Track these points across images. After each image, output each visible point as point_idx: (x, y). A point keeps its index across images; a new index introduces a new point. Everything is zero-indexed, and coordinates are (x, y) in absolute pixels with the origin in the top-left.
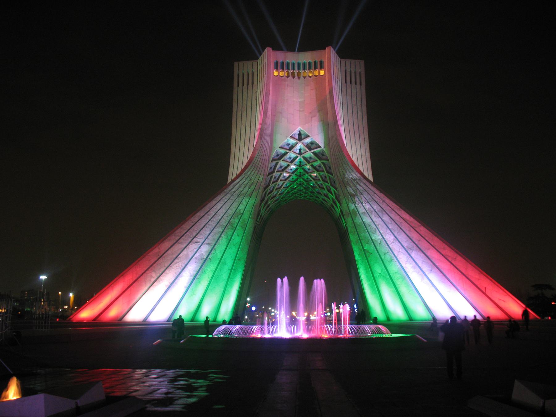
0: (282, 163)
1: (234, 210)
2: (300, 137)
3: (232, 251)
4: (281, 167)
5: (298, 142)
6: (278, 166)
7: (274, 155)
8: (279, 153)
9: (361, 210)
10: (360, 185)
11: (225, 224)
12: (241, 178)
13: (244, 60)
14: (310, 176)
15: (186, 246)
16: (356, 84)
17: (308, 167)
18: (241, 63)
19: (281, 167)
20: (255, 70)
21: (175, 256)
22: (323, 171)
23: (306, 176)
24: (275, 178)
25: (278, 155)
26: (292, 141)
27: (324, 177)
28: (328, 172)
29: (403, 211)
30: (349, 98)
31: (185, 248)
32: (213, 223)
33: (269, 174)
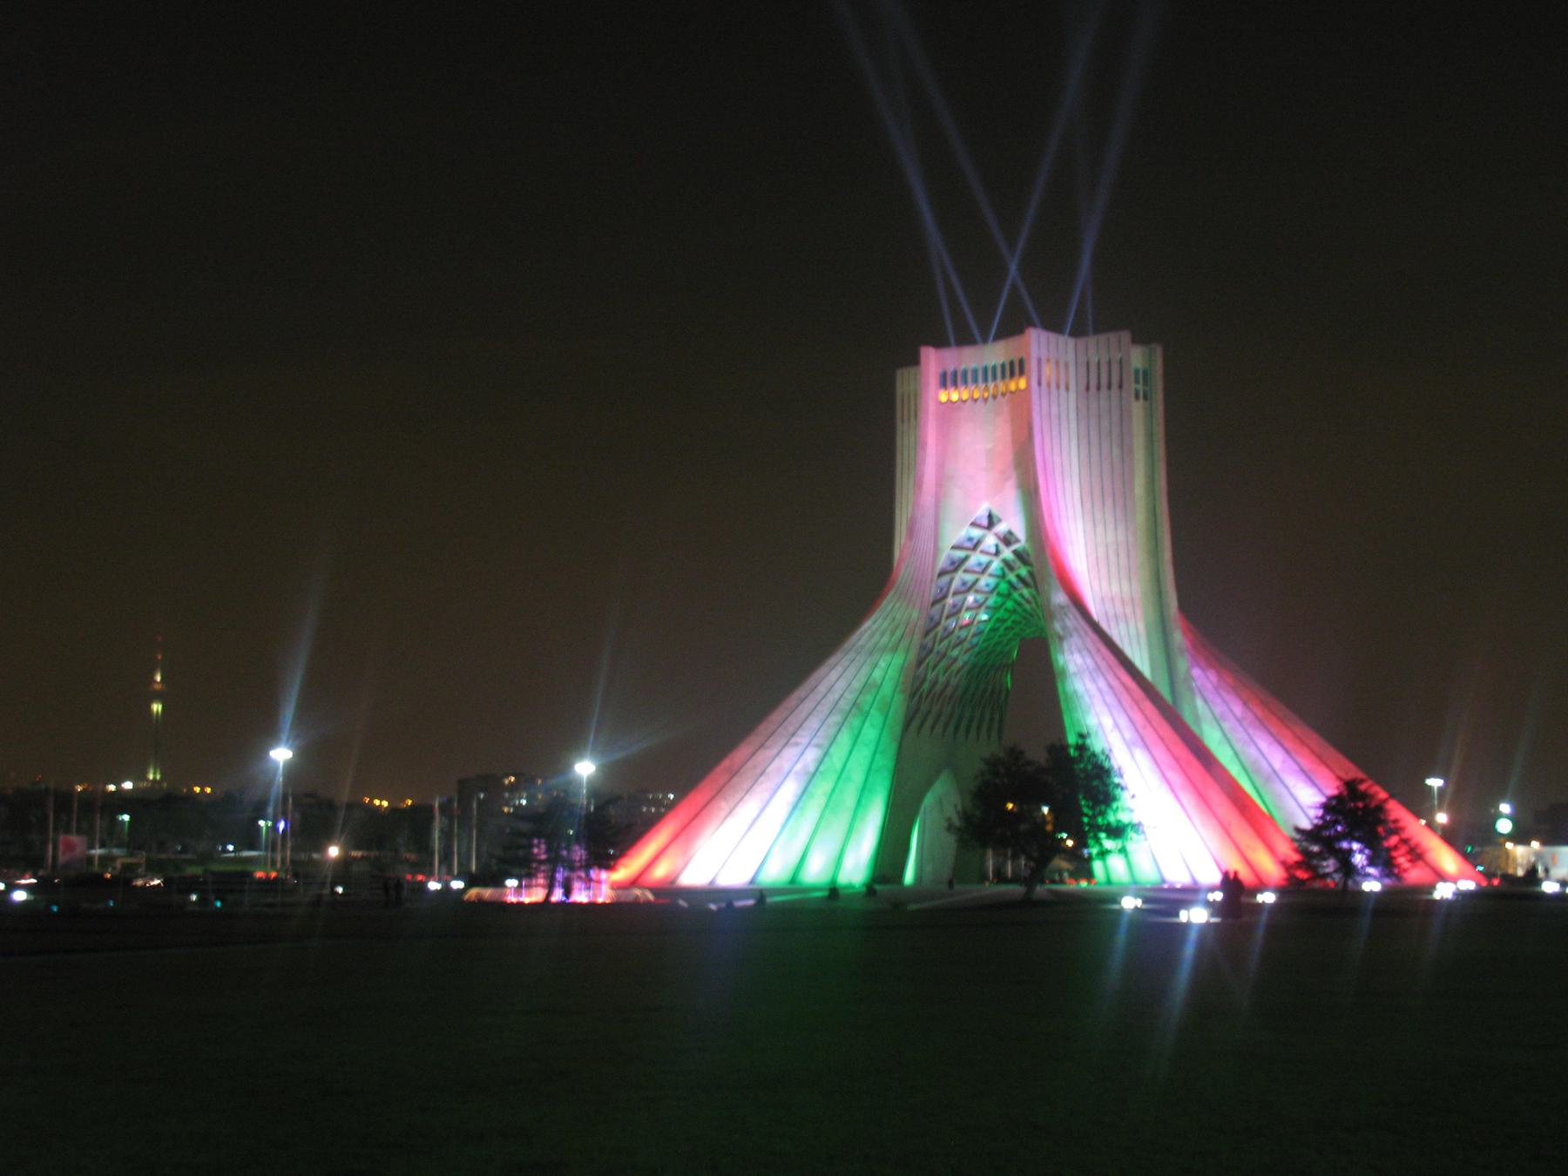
0: (960, 576)
2: (991, 521)
3: (863, 755)
4: (964, 583)
6: (955, 584)
7: (942, 562)
9: (1072, 668)
11: (847, 708)
25: (953, 563)
26: (976, 533)
30: (1093, 421)
32: (825, 708)
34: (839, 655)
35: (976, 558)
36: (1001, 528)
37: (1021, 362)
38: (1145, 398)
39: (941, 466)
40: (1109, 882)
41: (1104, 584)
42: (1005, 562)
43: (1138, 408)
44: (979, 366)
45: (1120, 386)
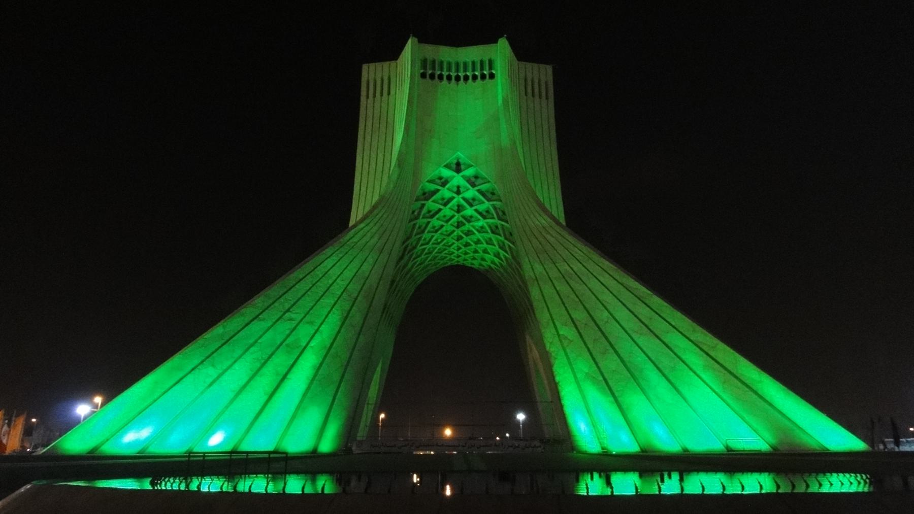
1: (355, 271)
5: (455, 174)
6: (424, 211)
7: (419, 192)
8: (426, 190)
9: (554, 273)
10: (552, 235)
12: (367, 221)
13: (375, 62)
14: (473, 227)
15: (272, 326)
16: (540, 97)
17: (469, 211)
18: (372, 66)
19: (429, 212)
20: (392, 74)
21: (251, 341)
22: (493, 218)
23: (467, 227)
24: (420, 227)
25: (424, 194)
26: (446, 173)
27: (494, 228)
28: (500, 219)
33: (411, 221)
35: (445, 193)
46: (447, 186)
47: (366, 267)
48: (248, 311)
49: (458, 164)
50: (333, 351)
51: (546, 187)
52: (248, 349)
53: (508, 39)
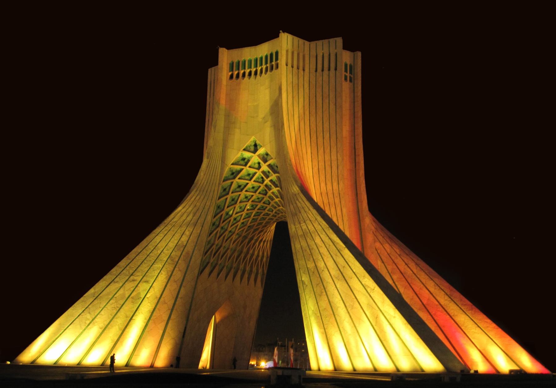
1: (176, 242)
2: (256, 147)
5: (252, 154)
6: (234, 186)
8: (234, 171)
10: (299, 202)
11: (165, 259)
15: (123, 285)
21: (111, 297)
25: (233, 174)
26: (247, 155)
29: (331, 231)
31: (121, 287)
34: (162, 226)
35: (247, 170)
36: (261, 151)
37: (277, 53)
38: (351, 81)
39: (228, 116)
40: (319, 370)
41: (323, 185)
42: (263, 172)
43: (346, 86)
44: (253, 58)
45: (336, 69)
46: (249, 165)
47: (184, 239)
48: (107, 278)
49: (256, 145)
50: (162, 299)
51: (328, 151)
52: (109, 301)
53: (284, 32)
